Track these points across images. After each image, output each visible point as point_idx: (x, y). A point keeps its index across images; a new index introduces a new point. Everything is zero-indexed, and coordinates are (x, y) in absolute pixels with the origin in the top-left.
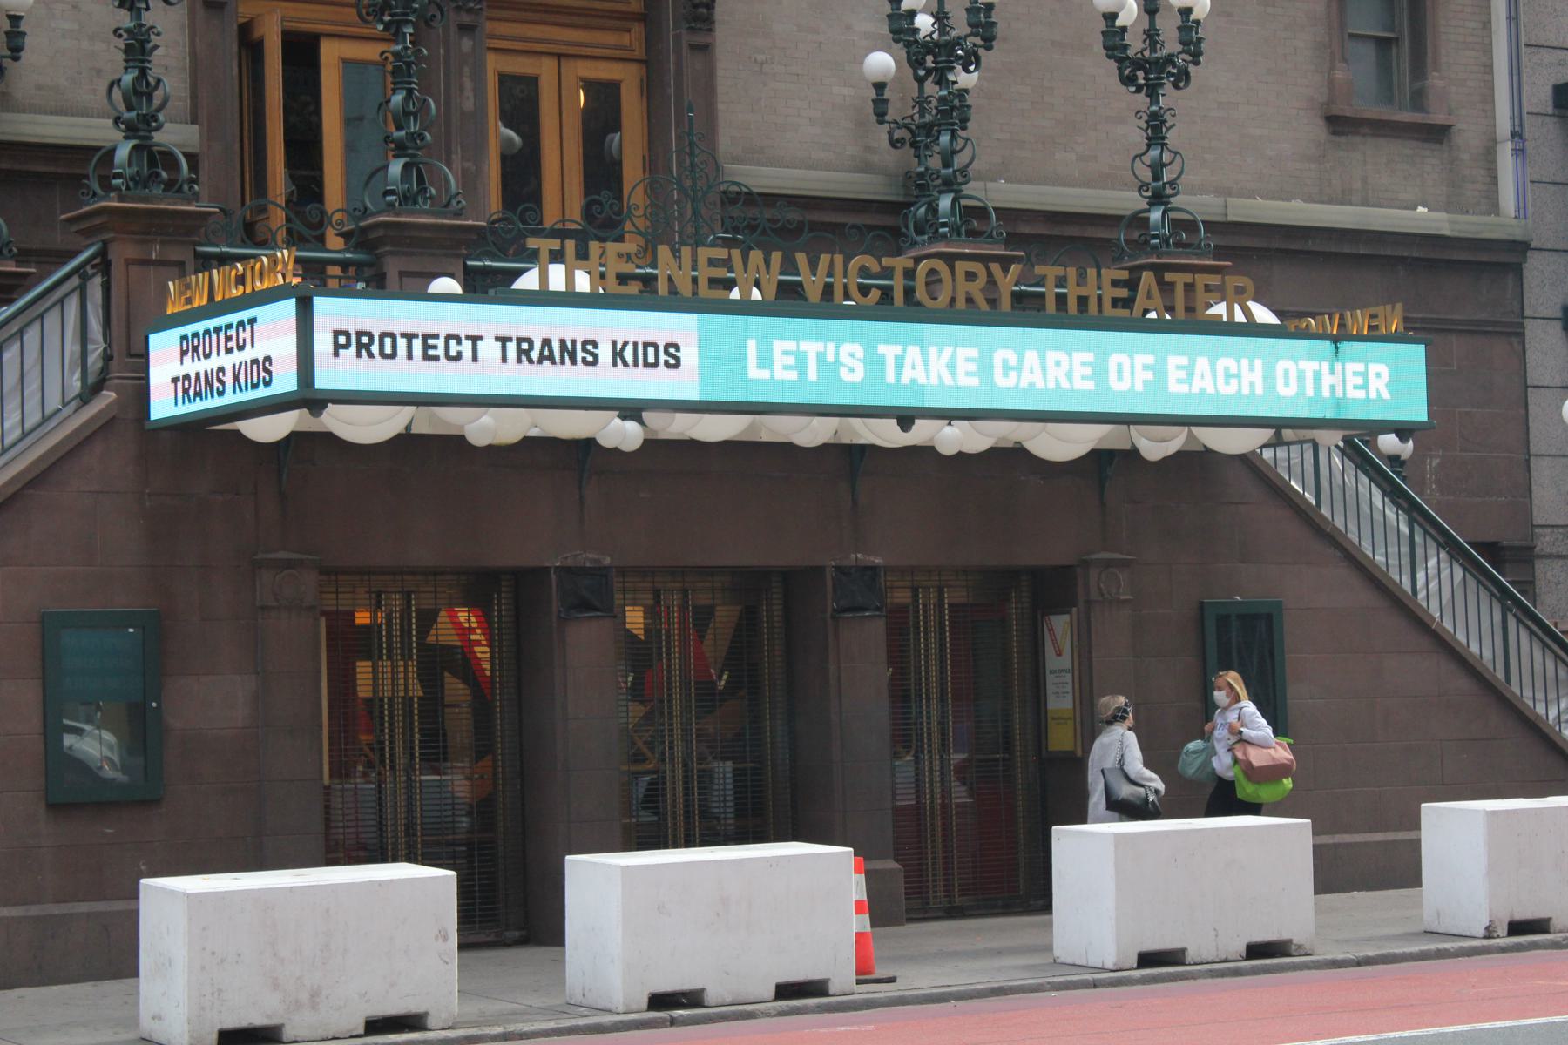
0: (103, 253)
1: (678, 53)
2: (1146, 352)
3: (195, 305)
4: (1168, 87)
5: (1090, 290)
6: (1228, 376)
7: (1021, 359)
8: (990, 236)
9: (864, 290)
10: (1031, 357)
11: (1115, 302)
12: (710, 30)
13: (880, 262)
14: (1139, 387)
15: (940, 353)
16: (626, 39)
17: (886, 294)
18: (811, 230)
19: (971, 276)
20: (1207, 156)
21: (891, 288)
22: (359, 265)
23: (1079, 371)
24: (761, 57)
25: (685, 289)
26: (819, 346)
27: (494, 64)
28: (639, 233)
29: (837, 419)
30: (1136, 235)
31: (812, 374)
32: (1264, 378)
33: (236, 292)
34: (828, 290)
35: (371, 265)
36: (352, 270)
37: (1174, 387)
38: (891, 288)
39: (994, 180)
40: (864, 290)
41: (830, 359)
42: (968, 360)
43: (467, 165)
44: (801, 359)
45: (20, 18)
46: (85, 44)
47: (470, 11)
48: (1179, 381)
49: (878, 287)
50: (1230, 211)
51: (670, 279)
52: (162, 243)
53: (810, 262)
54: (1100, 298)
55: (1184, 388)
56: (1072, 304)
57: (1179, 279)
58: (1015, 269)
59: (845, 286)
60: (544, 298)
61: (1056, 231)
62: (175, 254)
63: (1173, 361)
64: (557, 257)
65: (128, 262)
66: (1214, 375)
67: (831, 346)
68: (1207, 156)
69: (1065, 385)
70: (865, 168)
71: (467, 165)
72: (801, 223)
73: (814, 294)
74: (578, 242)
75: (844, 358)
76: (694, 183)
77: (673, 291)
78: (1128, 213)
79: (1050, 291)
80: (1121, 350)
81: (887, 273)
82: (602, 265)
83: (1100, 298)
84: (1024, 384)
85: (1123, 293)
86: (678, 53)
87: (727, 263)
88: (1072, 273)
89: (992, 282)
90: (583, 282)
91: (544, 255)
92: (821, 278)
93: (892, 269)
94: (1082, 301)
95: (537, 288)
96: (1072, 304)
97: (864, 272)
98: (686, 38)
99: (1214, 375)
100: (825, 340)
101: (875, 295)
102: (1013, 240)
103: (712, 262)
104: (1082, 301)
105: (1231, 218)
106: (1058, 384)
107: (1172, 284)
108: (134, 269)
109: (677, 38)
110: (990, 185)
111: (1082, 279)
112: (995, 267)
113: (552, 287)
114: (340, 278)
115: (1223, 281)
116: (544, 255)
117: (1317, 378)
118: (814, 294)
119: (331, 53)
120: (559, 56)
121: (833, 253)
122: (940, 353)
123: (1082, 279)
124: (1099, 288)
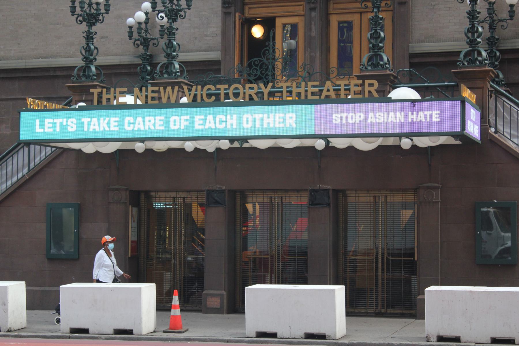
2: (200, 114)
5: (302, 90)
6: (221, 121)
7: (135, 120)
10: (139, 119)
11: (313, 94)
14: (183, 127)
15: (104, 120)
23: (158, 123)
26: (61, 120)
29: (121, 143)
31: (58, 129)
32: (237, 121)
37: (197, 127)
41: (65, 124)
42: (115, 121)
44: (54, 124)
48: (200, 124)
52: (86, 95)
55: (202, 127)
63: (197, 117)
66: (215, 122)
67: (65, 120)
69: (152, 128)
75: (69, 123)
80: (248, 113)
84: (136, 128)
85: (360, 89)
87: (158, 92)
95: (133, 103)
99: (215, 122)
100: (63, 118)
101: (213, 98)
103: (153, 92)
106: (104, 128)
117: (262, 120)
119: (279, 22)
122: (104, 120)
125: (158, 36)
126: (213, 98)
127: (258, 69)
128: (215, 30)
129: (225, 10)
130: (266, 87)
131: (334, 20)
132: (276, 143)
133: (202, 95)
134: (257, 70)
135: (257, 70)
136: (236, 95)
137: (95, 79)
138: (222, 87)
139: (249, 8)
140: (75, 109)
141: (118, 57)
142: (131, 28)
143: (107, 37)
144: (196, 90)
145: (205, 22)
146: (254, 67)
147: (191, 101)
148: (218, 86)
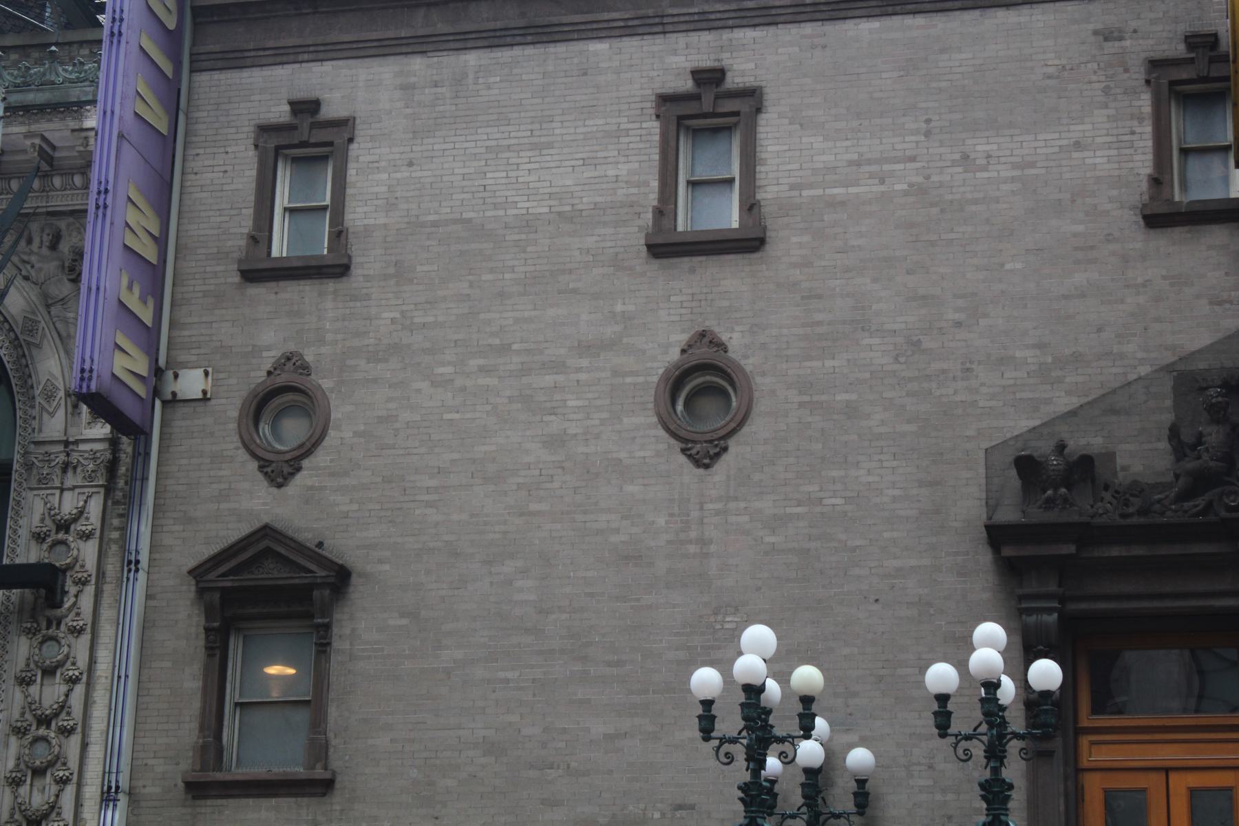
45: (865, 781)
46: (938, 797)
125: (850, 806)
131: (1094, 786)
139: (1092, 743)
143: (692, 807)
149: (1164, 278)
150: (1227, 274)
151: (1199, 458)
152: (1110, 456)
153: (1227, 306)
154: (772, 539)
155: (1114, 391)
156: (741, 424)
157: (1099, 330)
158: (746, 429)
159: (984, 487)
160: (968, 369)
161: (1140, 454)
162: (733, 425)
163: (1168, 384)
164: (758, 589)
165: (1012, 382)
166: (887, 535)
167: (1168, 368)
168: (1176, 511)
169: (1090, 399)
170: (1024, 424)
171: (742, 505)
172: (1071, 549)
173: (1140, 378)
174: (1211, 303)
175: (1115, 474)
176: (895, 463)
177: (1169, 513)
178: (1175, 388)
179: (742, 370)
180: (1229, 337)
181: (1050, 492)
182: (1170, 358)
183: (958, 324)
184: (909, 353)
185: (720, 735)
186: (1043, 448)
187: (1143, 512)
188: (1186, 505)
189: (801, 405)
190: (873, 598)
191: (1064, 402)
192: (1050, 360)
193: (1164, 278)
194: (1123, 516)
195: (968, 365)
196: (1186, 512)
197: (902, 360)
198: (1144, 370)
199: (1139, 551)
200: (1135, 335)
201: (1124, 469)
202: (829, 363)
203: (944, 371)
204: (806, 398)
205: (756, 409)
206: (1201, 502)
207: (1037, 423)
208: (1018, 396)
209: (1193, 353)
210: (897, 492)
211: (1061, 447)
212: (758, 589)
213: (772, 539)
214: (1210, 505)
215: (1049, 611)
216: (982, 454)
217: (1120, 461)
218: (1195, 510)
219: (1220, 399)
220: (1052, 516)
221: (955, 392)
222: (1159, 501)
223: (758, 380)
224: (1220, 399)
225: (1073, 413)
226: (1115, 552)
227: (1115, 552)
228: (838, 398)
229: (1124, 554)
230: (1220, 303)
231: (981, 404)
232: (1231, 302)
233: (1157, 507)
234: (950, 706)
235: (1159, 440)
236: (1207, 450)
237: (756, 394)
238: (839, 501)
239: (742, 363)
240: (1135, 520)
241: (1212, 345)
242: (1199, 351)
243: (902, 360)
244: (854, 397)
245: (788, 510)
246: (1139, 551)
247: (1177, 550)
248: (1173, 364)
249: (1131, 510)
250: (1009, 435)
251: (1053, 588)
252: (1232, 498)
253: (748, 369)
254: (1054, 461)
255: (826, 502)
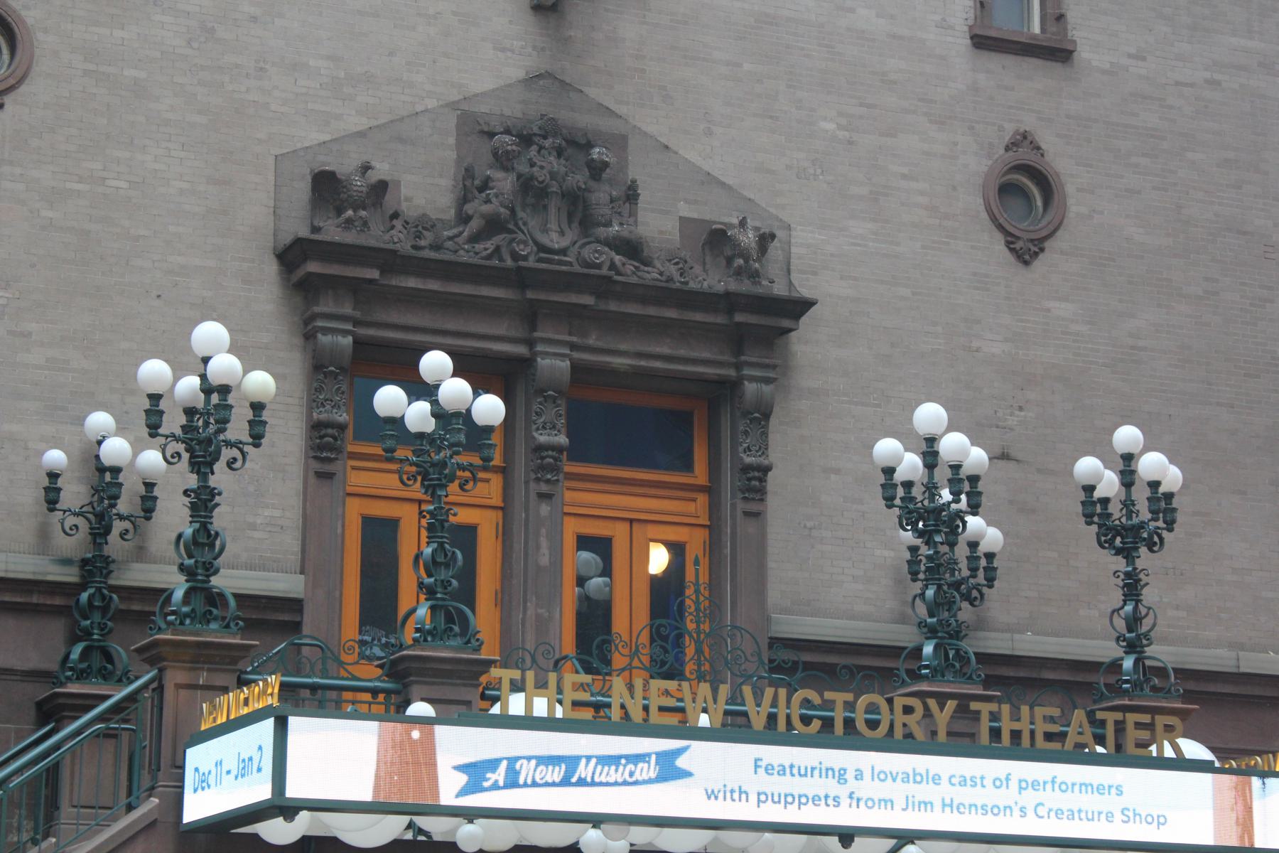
0: (159, 678)
1: (733, 517)
3: (219, 722)
4: (1143, 550)
8: (970, 678)
9: (806, 720)
12: (762, 500)
13: (822, 696)
16: (691, 507)
17: (828, 724)
18: (805, 669)
19: (908, 710)
20: (1222, 615)
21: (832, 719)
22: (387, 692)
24: (809, 524)
25: (637, 715)
27: (572, 528)
28: (645, 669)
30: (1112, 679)
33: (246, 711)
34: (772, 718)
35: (397, 692)
36: (381, 697)
38: (832, 719)
39: (1019, 632)
40: (806, 720)
43: (540, 611)
45: (153, 485)
47: (548, 481)
49: (819, 718)
50: (1242, 664)
51: (623, 706)
52: (209, 670)
53: (754, 693)
54: (1032, 732)
56: (1006, 736)
57: (1111, 717)
58: (951, 705)
59: (788, 717)
60: (528, 722)
61: (1079, 678)
62: (220, 680)
64: (517, 687)
65: (179, 686)
68: (1222, 615)
70: (902, 619)
71: (540, 611)
72: (795, 663)
73: (758, 722)
74: (540, 669)
76: (698, 626)
77: (626, 716)
78: (1107, 660)
79: (839, 715)
81: (829, 705)
82: (644, 698)
83: (1032, 732)
86: (733, 517)
88: (1006, 708)
89: (928, 714)
90: (541, 707)
91: (506, 685)
92: (766, 708)
93: (833, 702)
94: (1016, 735)
96: (1006, 736)
97: (806, 703)
98: (741, 506)
102: (988, 682)
104: (1016, 735)
105: (1243, 670)
107: (978, 712)
108: (183, 692)
109: (733, 506)
110: (1017, 636)
111: (1016, 717)
112: (932, 703)
113: (536, 714)
114: (370, 704)
115: (1153, 718)
116: (506, 685)
118: (758, 722)
120: (631, 521)
121: (777, 687)
123: (1016, 717)
124: (1032, 723)
126: (816, 724)
127: (669, 647)
128: (277, 513)
129: (316, 466)
130: (942, 710)
132: (716, 839)
133: (788, 717)
134: (666, 651)
135: (666, 651)
136: (873, 725)
137: (1126, 691)
138: (840, 697)
139: (354, 468)
140: (1161, 763)
141: (861, 624)
142: (53, 476)
144: (774, 704)
145: (251, 489)
146: (660, 642)
147: (718, 725)
148: (828, 695)
149: (455, 13)
150: (510, 22)
151: (488, 201)
152: (398, 183)
153: (509, 54)
154: (50, 214)
155: (402, 119)
156: (20, 82)
157: (391, 54)
158: (23, 88)
159: (272, 195)
160: (261, 69)
161: (425, 187)
162: (12, 81)
163: (451, 121)
164: (33, 266)
165: (304, 90)
166: (172, 228)
167: (453, 106)
168: (468, 251)
169: (376, 123)
170: (315, 136)
171: (18, 171)
172: (374, 274)
173: (426, 111)
174: (495, 49)
175: (399, 203)
176: (183, 154)
177: (462, 252)
178: (458, 127)
179: (23, 22)
180: (509, 85)
181: (350, 212)
182: (455, 96)
183: (254, 19)
184: (202, 39)
185: (167, 432)
186: (345, 165)
187: (436, 247)
188: (479, 247)
189: (86, 73)
190: (155, 293)
191: (356, 123)
192: (342, 75)
193: (455, 13)
194: (415, 247)
195: (262, 64)
196: (477, 253)
197: (195, 45)
198: (431, 103)
199: (433, 285)
200: (424, 65)
201: (408, 199)
202: (118, 33)
203: (237, 66)
204: (91, 67)
205: (36, 69)
206: (490, 245)
207: (327, 137)
208: (310, 106)
209: (476, 95)
210: (185, 186)
211: (366, 168)
212: (33, 266)
213: (50, 214)
214: (498, 249)
215: (345, 333)
216: (271, 161)
217: (404, 191)
218: (485, 253)
219: (514, 147)
220: (350, 238)
221: (248, 90)
222: (450, 238)
223: (40, 36)
224: (514, 147)
225: (361, 134)
226: (412, 282)
227: (412, 282)
228: (126, 73)
229: (420, 286)
230: (503, 50)
231: (273, 107)
232: (513, 51)
233: (449, 244)
234: (265, 415)
235: (441, 176)
236: (497, 196)
237: (37, 52)
238: (123, 184)
239: (23, 13)
240: (428, 254)
241: (493, 90)
242: (484, 94)
243: (195, 45)
244: (143, 75)
245: (68, 185)
246: (433, 285)
247: (467, 289)
248: (458, 102)
249: (423, 243)
250: (299, 146)
251: (348, 310)
252: (522, 246)
253: (30, 21)
254: (358, 182)
255: (109, 182)
